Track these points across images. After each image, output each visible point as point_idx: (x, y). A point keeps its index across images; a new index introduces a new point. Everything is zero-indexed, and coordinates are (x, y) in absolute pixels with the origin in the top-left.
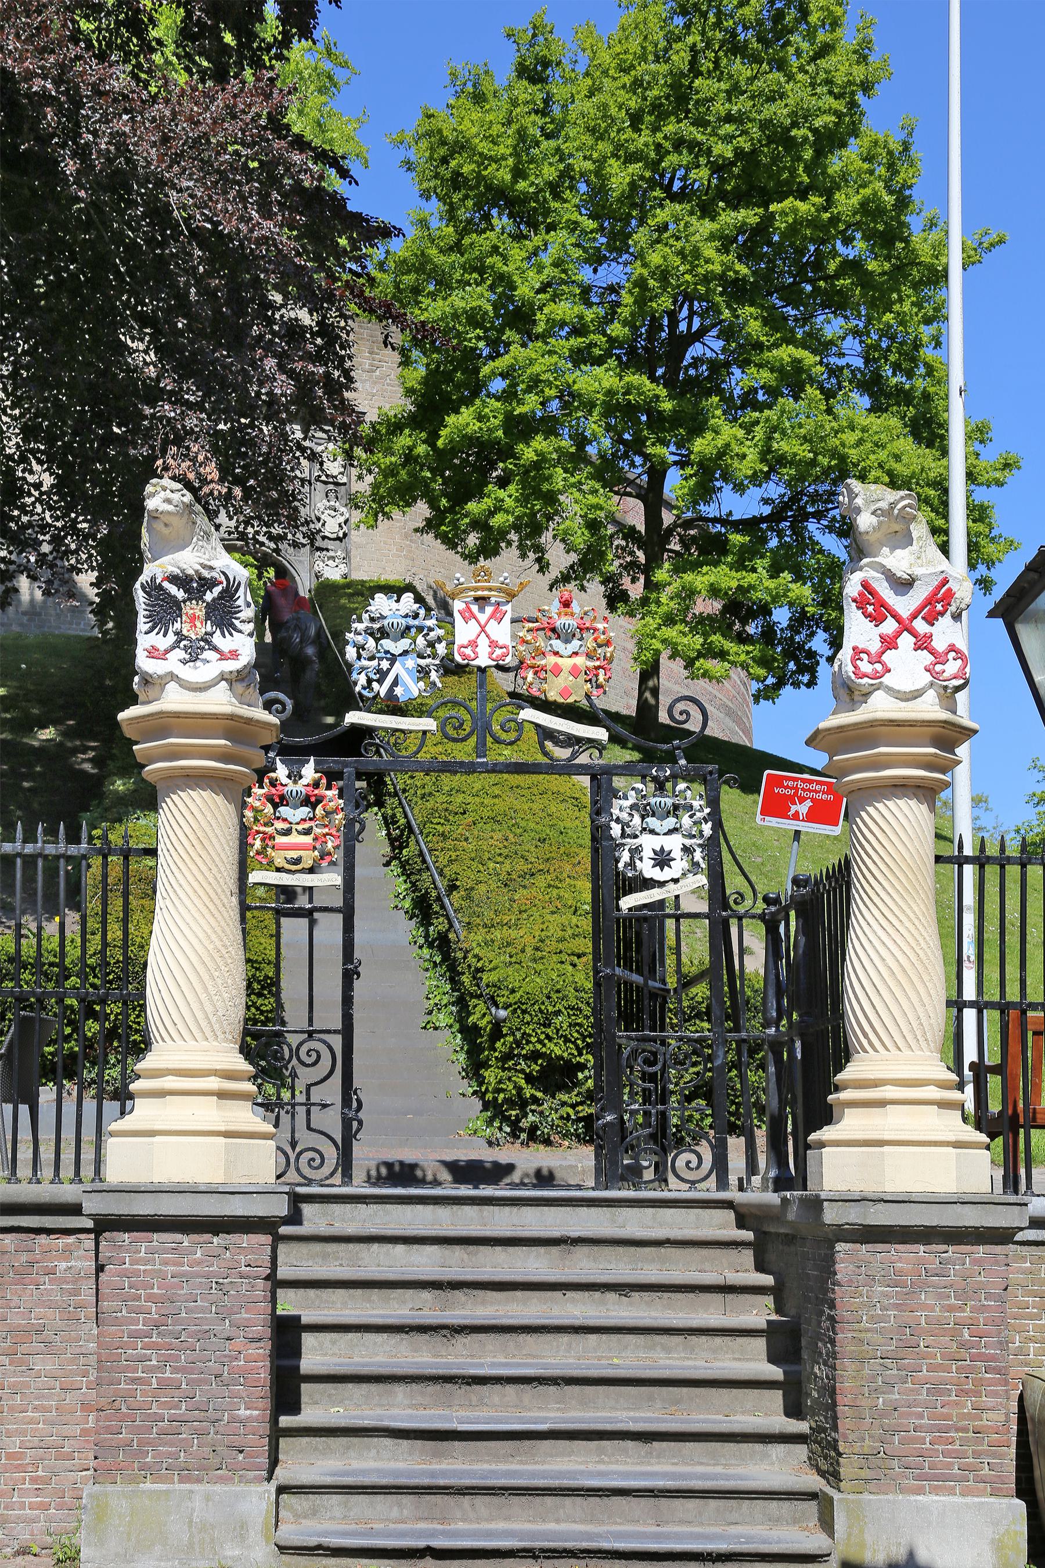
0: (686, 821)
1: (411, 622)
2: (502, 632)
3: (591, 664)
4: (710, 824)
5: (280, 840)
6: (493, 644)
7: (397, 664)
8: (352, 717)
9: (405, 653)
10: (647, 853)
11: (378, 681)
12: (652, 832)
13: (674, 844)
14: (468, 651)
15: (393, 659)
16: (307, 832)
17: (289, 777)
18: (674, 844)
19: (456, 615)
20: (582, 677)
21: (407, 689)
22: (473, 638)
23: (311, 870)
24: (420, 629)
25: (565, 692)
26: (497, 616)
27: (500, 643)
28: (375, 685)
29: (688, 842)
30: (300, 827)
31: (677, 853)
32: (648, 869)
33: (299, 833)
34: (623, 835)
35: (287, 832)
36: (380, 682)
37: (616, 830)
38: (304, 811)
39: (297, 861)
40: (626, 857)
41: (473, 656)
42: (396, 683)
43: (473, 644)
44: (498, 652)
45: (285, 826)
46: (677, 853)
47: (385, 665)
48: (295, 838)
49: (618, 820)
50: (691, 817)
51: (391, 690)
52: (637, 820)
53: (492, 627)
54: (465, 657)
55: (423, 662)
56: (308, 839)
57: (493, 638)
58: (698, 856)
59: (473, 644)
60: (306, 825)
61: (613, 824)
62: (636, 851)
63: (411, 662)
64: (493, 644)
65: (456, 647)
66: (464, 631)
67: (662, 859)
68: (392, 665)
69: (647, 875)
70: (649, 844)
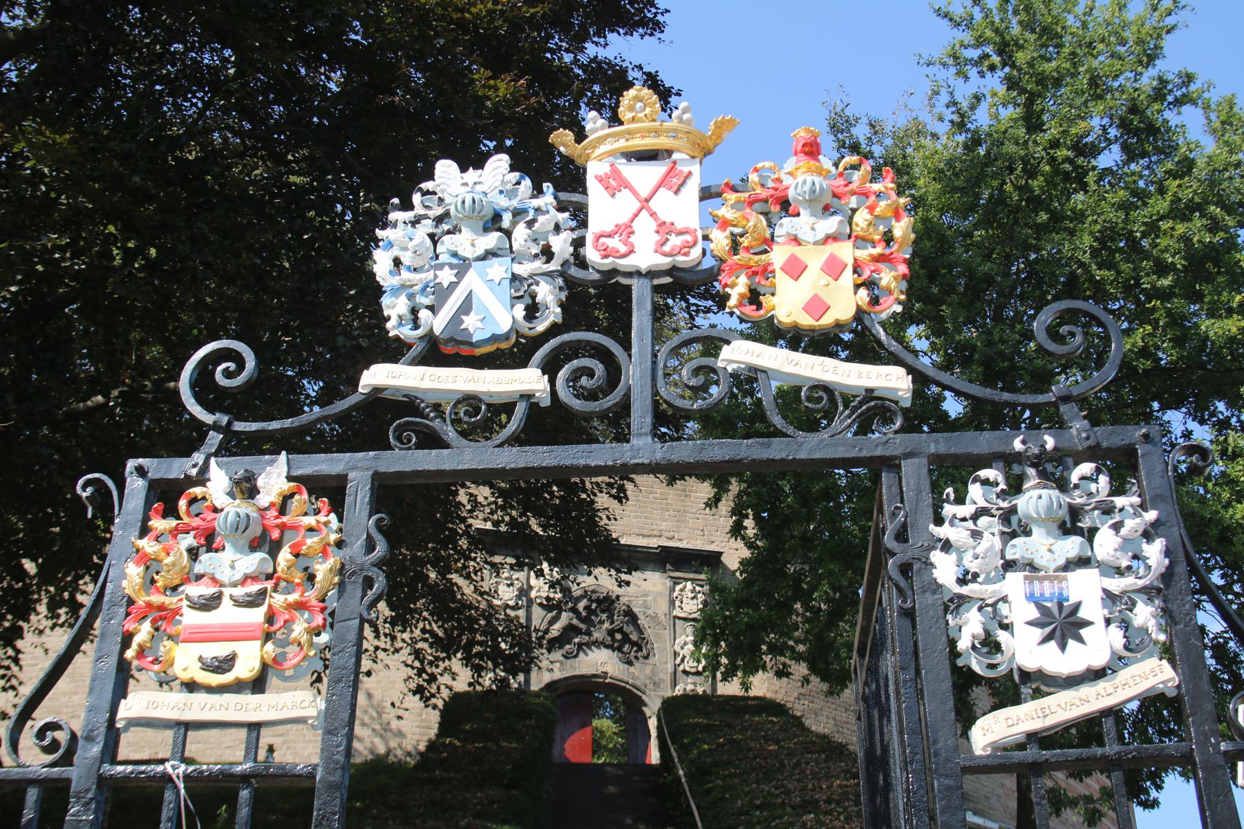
0: (1106, 544)
1: (503, 202)
2: (683, 208)
3: (864, 254)
5: (191, 618)
8: (377, 376)
9: (489, 254)
10: (1021, 611)
11: (431, 308)
14: (615, 243)
15: (462, 266)
17: (231, 494)
19: (591, 183)
20: (848, 278)
22: (624, 219)
23: (258, 685)
24: (518, 213)
25: (816, 305)
27: (679, 225)
28: (424, 314)
29: (1116, 584)
30: (240, 592)
31: (1093, 610)
32: (1026, 649)
33: (239, 603)
37: (944, 569)
38: (253, 561)
39: (225, 664)
42: (466, 306)
43: (626, 230)
44: (675, 241)
45: (210, 590)
47: (446, 276)
48: (227, 614)
49: (947, 546)
50: (1117, 527)
51: (456, 319)
53: (665, 204)
55: (523, 269)
56: (257, 615)
57: (664, 217)
58: (1144, 614)
59: (626, 230)
60: (254, 588)
61: (936, 556)
64: (666, 229)
66: (604, 209)
68: (460, 275)
69: (1030, 664)
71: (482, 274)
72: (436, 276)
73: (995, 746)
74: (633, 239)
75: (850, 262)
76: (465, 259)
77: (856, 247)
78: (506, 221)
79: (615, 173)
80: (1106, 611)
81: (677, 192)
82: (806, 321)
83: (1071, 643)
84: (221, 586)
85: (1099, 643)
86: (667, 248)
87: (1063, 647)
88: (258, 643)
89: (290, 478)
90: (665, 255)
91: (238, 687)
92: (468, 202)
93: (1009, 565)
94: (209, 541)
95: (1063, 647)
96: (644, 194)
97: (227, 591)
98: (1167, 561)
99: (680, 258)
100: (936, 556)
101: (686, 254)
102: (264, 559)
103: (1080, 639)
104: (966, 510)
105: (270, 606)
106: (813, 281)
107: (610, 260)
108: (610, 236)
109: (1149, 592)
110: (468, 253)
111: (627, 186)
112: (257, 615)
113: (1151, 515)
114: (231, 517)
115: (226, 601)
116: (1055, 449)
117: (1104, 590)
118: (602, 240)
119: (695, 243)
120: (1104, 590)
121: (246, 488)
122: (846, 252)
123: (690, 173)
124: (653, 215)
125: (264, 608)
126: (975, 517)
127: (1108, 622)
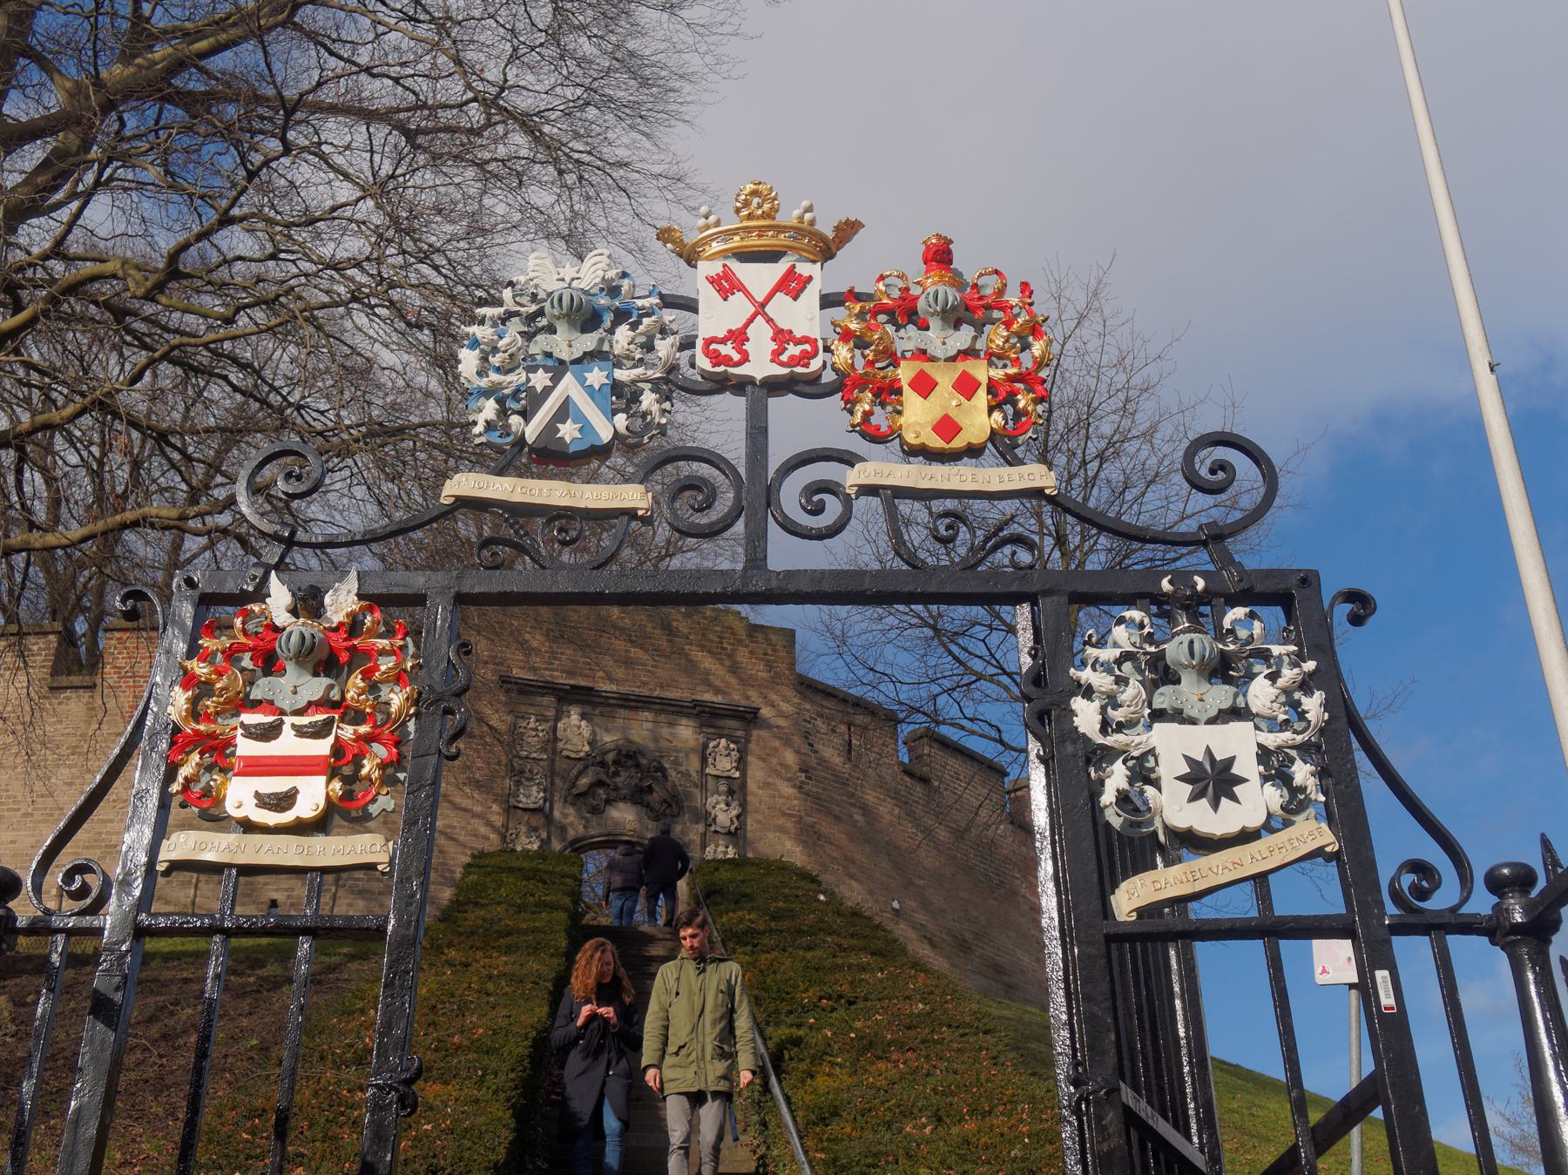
0: (1261, 694)
1: (603, 301)
4: (1319, 696)
5: (246, 747)
6: (782, 337)
7: (568, 379)
10: (1170, 767)
12: (1177, 716)
13: (1238, 744)
14: (727, 350)
15: (558, 369)
16: (319, 731)
17: (294, 612)
18: (1238, 744)
20: (982, 398)
21: (586, 427)
22: (737, 325)
25: (947, 427)
26: (792, 285)
29: (1272, 740)
31: (1247, 766)
32: (1175, 806)
33: (300, 732)
34: (1105, 727)
35: (269, 733)
36: (526, 415)
37: (1086, 716)
38: (315, 687)
39: (284, 801)
40: (1117, 778)
41: (736, 357)
42: (565, 411)
43: (738, 337)
44: (793, 350)
46: (1247, 766)
47: (540, 380)
48: (288, 744)
50: (1273, 677)
51: (550, 429)
52: (1133, 691)
54: (717, 358)
55: (622, 375)
56: (322, 747)
58: (1302, 772)
59: (738, 337)
60: (320, 717)
61: (1078, 703)
62: (1143, 773)
63: (596, 377)
64: (782, 337)
65: (699, 343)
67: (1213, 780)
68: (556, 380)
70: (1173, 747)
71: (582, 380)
72: (528, 380)
73: (1142, 912)
74: (747, 346)
75: (984, 380)
76: (562, 362)
77: (991, 364)
78: (608, 319)
79: (727, 275)
80: (1261, 768)
81: (795, 298)
82: (936, 442)
83: (1224, 801)
84: (283, 713)
85: (1256, 800)
86: (784, 358)
87: (1215, 805)
88: (323, 779)
89: (360, 596)
90: (782, 364)
91: (300, 828)
92: (566, 301)
93: (1158, 715)
94: (269, 663)
95: (1215, 805)
96: (760, 299)
97: (289, 720)
98: (1326, 716)
99: (799, 370)
100: (1078, 703)
101: (806, 365)
102: (331, 687)
103: (1234, 798)
104: (1108, 654)
105: (337, 738)
106: (945, 398)
107: (722, 368)
108: (723, 341)
109: (1305, 749)
110: (565, 355)
111: (742, 288)
112: (322, 747)
113: (1310, 665)
114: (295, 639)
115: (287, 728)
116: (1206, 590)
117: (1260, 746)
118: (713, 346)
119: (815, 354)
120: (1260, 746)
121: (309, 603)
122: (981, 371)
123: (810, 278)
124: (769, 320)
125: (331, 740)
126: (1119, 662)
127: (1265, 779)
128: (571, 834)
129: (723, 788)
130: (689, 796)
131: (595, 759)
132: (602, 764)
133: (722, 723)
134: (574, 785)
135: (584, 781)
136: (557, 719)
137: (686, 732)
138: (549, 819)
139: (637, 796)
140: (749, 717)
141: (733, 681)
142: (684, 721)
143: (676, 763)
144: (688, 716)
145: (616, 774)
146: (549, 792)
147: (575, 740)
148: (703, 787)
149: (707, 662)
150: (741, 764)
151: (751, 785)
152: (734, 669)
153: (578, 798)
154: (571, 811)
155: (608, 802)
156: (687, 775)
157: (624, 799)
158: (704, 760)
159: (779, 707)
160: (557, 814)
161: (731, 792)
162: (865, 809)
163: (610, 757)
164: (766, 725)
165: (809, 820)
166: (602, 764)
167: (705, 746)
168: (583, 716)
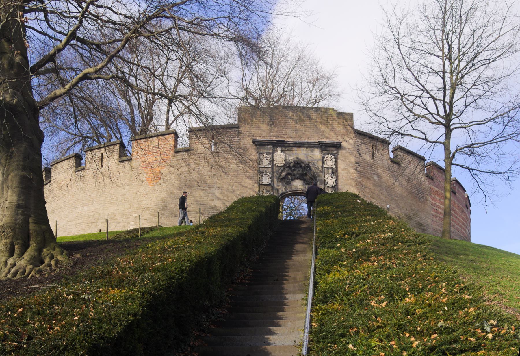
128: (281, 192)
129: (330, 172)
130: (319, 175)
131: (287, 166)
132: (289, 167)
133: (329, 149)
134: (280, 175)
135: (284, 174)
136: (273, 153)
137: (317, 154)
138: (273, 187)
139: (302, 177)
140: (338, 146)
141: (332, 133)
142: (316, 150)
143: (314, 164)
144: (317, 147)
145: (294, 170)
146: (272, 178)
147: (280, 159)
148: (323, 172)
149: (323, 128)
150: (336, 163)
151: (339, 170)
152: (333, 129)
153: (282, 180)
154: (280, 184)
155: (293, 180)
156: (317, 168)
157: (297, 178)
158: (323, 163)
159: (349, 142)
160: (275, 185)
161: (333, 173)
162: (378, 175)
163: (292, 164)
164: (344, 148)
165: (359, 180)
166: (289, 167)
167: (323, 158)
168: (282, 151)
